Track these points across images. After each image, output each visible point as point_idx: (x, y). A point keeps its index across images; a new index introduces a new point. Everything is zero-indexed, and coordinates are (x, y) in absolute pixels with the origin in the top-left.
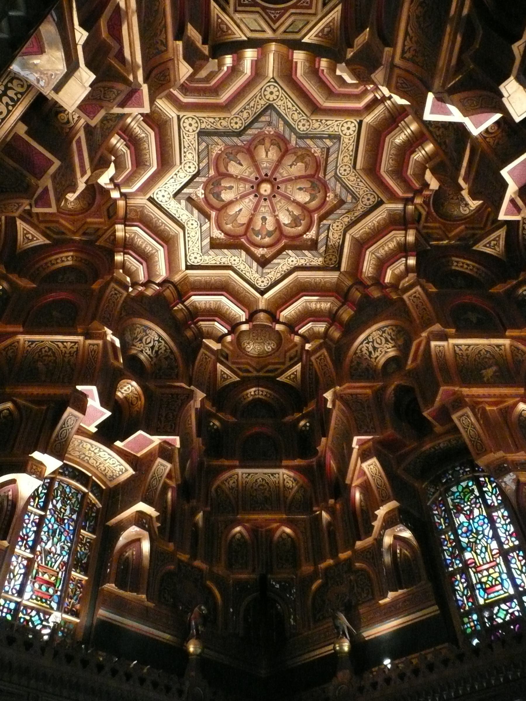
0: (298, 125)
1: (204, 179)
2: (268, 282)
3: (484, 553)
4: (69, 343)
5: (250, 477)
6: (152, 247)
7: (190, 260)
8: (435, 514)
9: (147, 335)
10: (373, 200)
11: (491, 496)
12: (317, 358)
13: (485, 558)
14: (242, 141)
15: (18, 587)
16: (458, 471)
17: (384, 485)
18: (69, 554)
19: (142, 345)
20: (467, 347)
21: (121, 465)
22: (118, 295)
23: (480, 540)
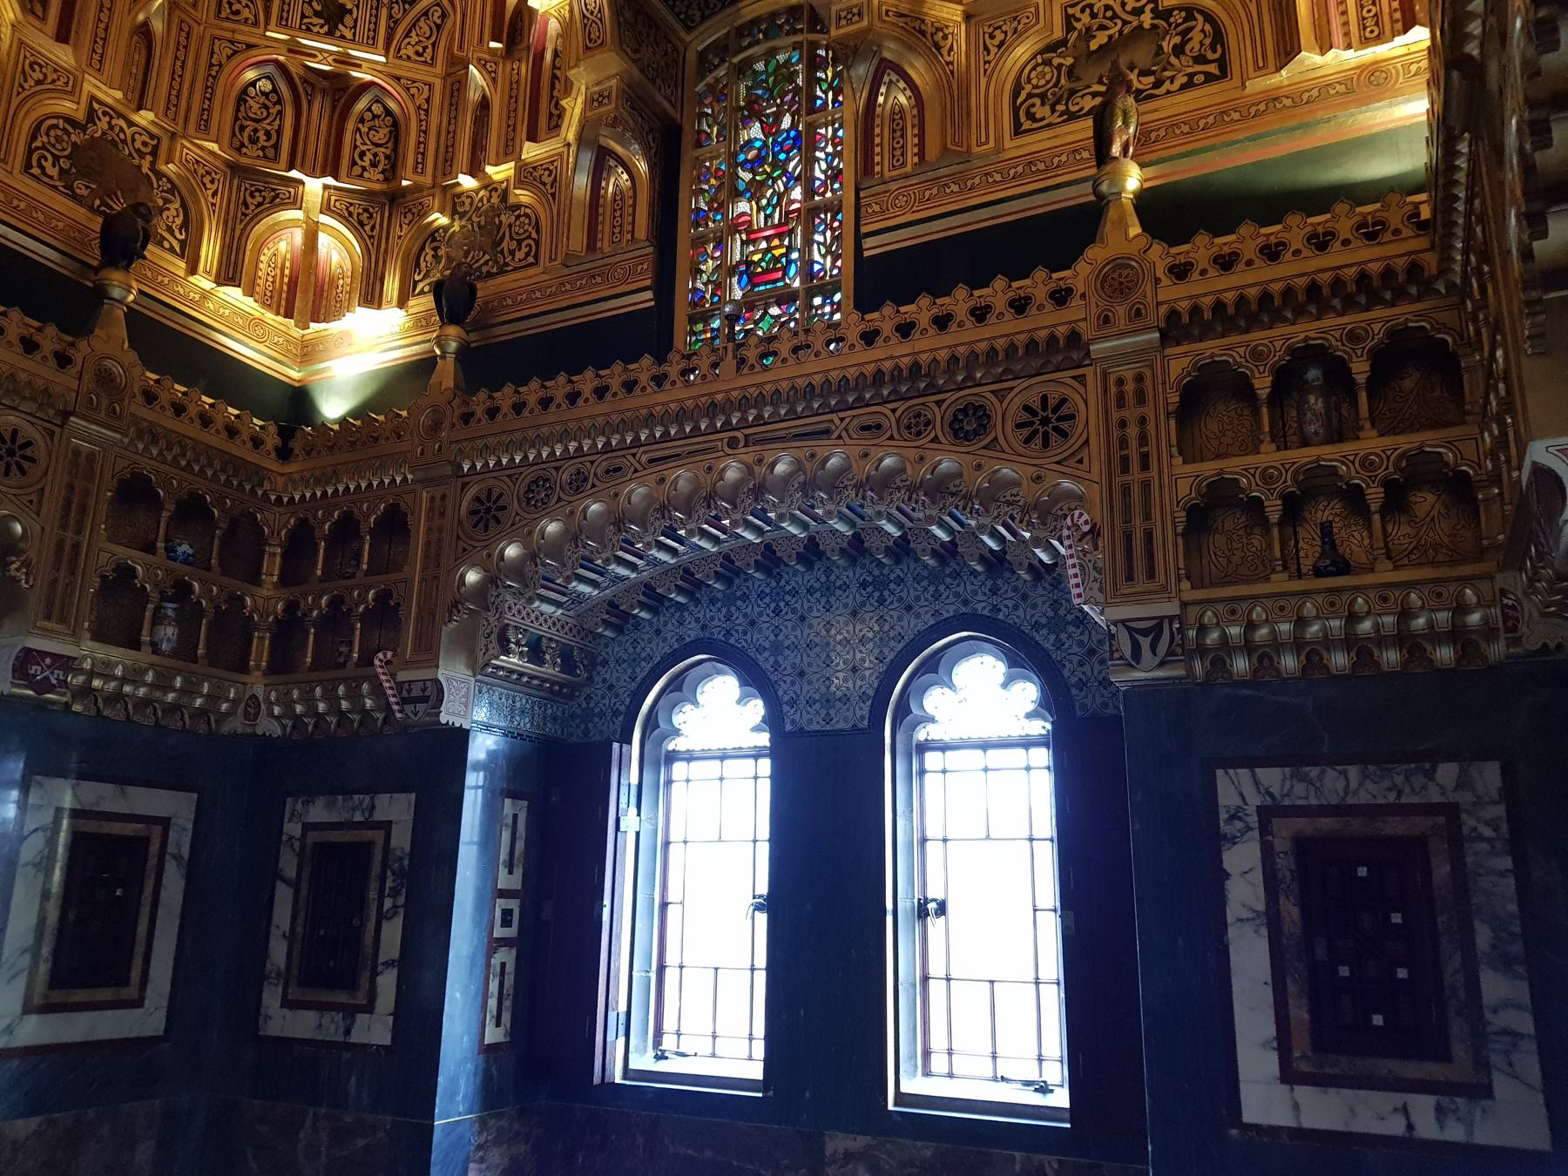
3: (774, 207)
8: (707, 114)
11: (825, 93)
23: (774, 180)
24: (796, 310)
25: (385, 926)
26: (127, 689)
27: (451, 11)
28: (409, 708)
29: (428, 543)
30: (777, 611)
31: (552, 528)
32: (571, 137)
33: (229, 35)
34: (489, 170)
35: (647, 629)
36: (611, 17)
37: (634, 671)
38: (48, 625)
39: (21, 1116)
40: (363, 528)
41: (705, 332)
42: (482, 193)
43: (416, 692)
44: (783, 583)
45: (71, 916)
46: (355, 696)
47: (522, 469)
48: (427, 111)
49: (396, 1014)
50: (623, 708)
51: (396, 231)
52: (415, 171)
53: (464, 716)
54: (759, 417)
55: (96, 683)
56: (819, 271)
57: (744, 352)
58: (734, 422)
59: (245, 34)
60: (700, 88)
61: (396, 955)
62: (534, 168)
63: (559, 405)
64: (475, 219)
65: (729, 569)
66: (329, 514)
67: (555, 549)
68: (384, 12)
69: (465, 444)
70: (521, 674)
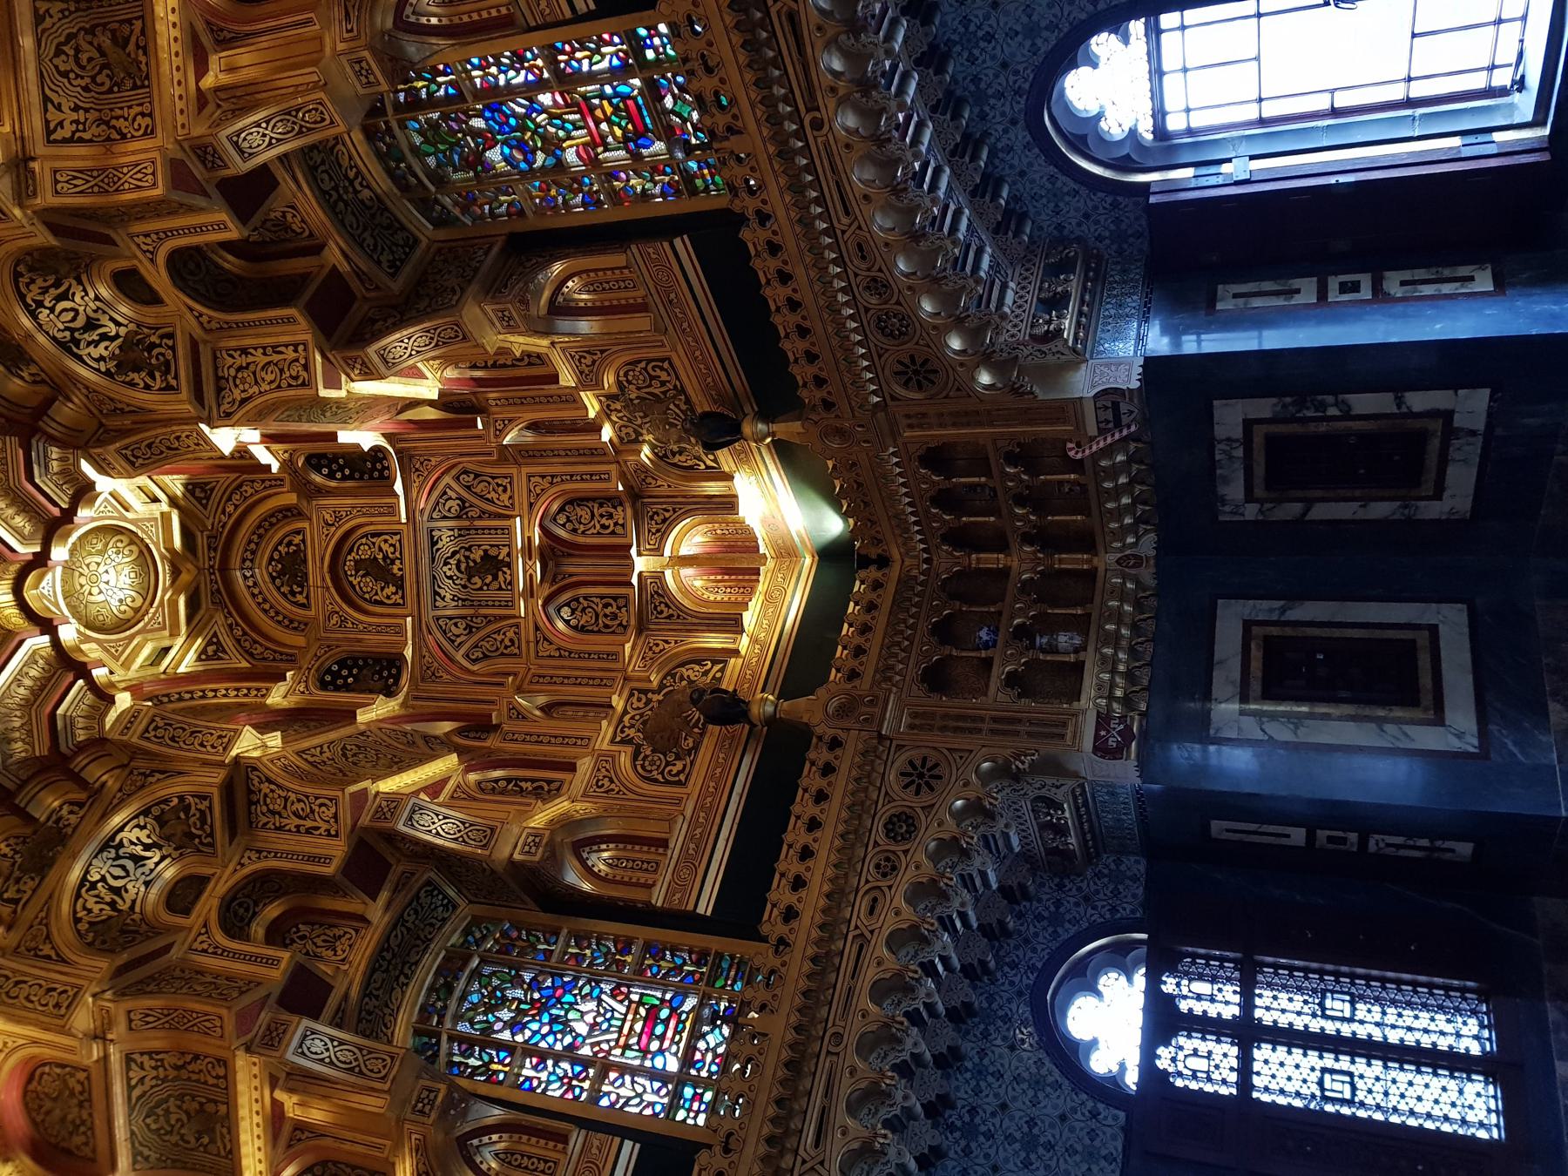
3: (564, 121)
4: (131, 1074)
5: (442, 592)
8: (491, 209)
9: (103, 879)
11: (439, 85)
12: (133, 464)
13: (573, 123)
15: (657, 1085)
18: (598, 983)
19: (129, 886)
20: (50, 106)
21: (417, 897)
24: (664, 77)
25: (1358, 409)
26: (1122, 668)
27: (461, 466)
28: (1125, 419)
29: (954, 425)
30: (989, 37)
31: (927, 306)
32: (545, 342)
33: (532, 645)
34: (592, 414)
35: (1019, 186)
36: (430, 320)
37: (1068, 194)
38: (1069, 736)
39: (1546, 715)
40: (946, 485)
41: (703, 176)
42: (615, 419)
43: (1109, 415)
44: (955, 37)
45: (1343, 694)
46: (1113, 472)
47: (871, 345)
48: (552, 477)
49: (1456, 387)
50: (1109, 199)
51: (664, 490)
52: (608, 480)
53: (1131, 365)
54: (786, 100)
55: (1119, 693)
56: (618, 58)
57: (720, 130)
58: (794, 127)
59: (528, 632)
61: (1390, 396)
62: (581, 373)
63: (804, 318)
64: (639, 421)
65: (945, 105)
66: (936, 518)
67: (948, 301)
68: (478, 523)
69: (853, 404)
70: (1081, 313)
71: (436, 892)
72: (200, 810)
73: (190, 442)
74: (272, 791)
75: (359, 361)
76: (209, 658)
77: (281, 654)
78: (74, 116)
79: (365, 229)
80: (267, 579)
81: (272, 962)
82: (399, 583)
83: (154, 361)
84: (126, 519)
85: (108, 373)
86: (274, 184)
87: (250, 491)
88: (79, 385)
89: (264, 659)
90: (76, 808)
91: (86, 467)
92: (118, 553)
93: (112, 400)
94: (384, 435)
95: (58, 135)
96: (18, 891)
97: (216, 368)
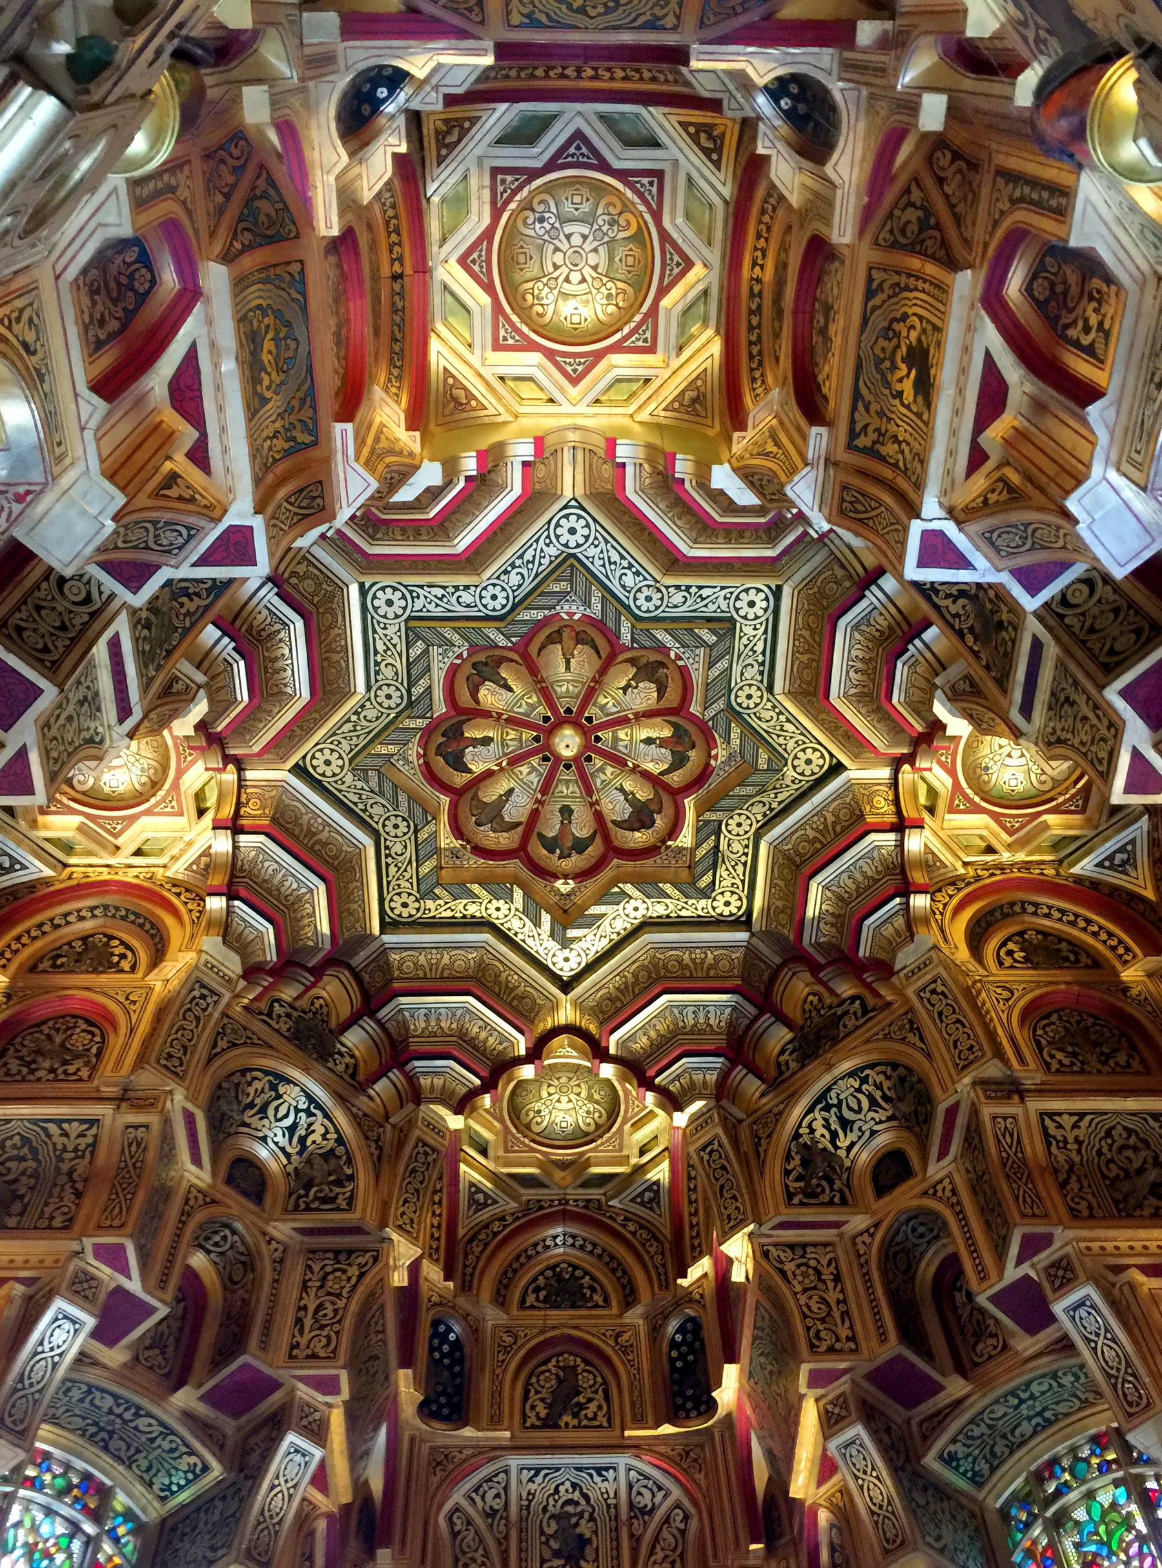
0: (635, 599)
1: (421, 723)
2: (578, 959)
4: (75, 1124)
5: (539, 1479)
6: (297, 880)
7: (392, 909)
9: (279, 1096)
10: (821, 762)
12: (704, 1148)
14: (508, 638)
16: (1086, 1460)
17: (889, 1503)
19: (266, 1122)
20: (1075, 1118)
21: (192, 1453)
22: (209, 1000)
60: (1017, 1557)
71: (190, 1476)
72: (336, 1198)
73: (731, 1210)
74: (349, 1279)
75: (844, 1413)
76: (471, 1195)
77: (472, 1275)
78: (1071, 1139)
79: (990, 1427)
80: (552, 1261)
81: (163, 1284)
82: (549, 1423)
83: (814, 1181)
84: (624, 1123)
85: (797, 1136)
86: (1032, 1329)
87: (652, 1250)
88: (781, 1107)
89: (466, 1255)
90: (350, 1071)
91: (697, 1106)
92: (588, 1112)
93: (770, 1136)
94: (729, 1415)
95: (1048, 1121)
96: (279, 1016)
97: (815, 1245)
